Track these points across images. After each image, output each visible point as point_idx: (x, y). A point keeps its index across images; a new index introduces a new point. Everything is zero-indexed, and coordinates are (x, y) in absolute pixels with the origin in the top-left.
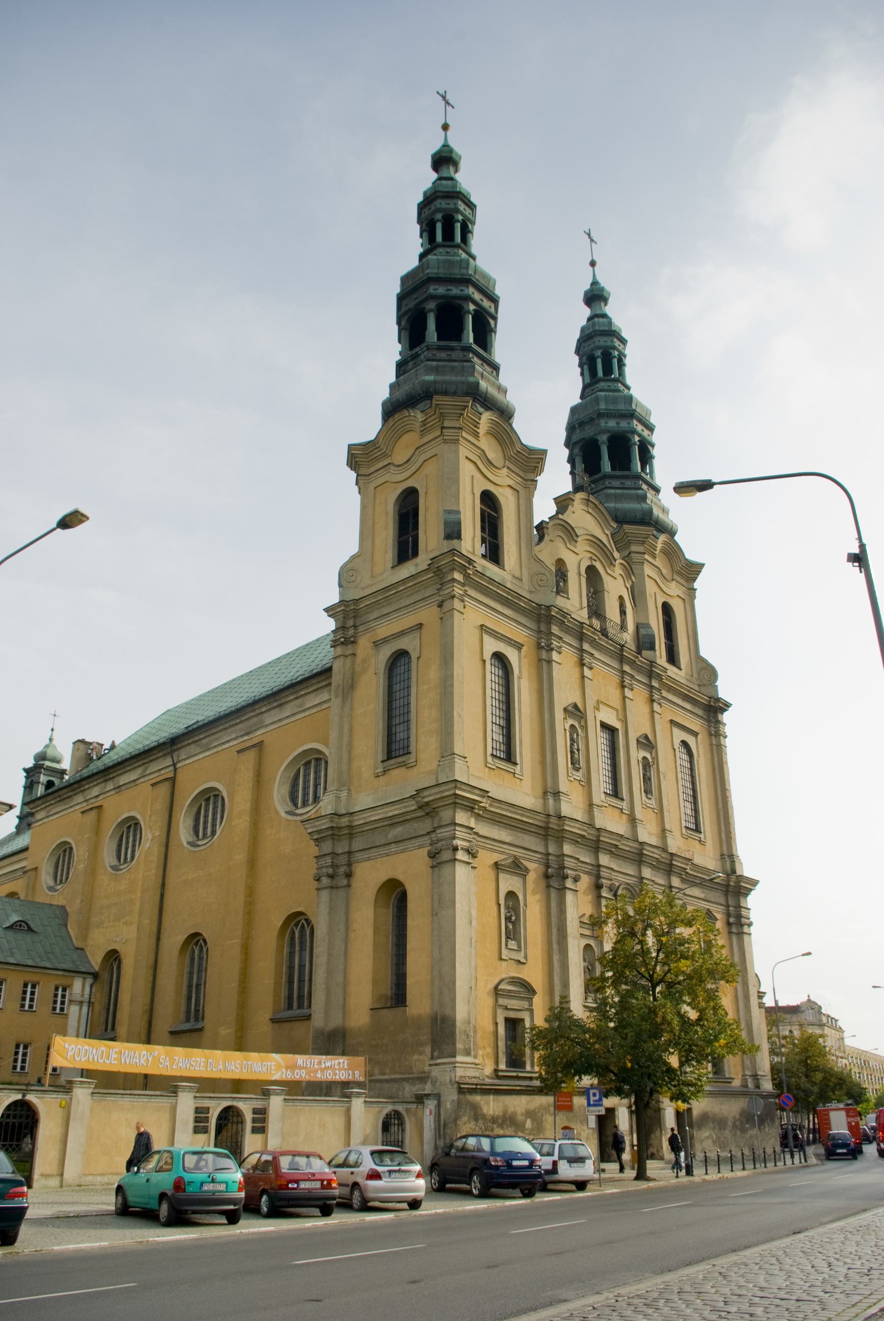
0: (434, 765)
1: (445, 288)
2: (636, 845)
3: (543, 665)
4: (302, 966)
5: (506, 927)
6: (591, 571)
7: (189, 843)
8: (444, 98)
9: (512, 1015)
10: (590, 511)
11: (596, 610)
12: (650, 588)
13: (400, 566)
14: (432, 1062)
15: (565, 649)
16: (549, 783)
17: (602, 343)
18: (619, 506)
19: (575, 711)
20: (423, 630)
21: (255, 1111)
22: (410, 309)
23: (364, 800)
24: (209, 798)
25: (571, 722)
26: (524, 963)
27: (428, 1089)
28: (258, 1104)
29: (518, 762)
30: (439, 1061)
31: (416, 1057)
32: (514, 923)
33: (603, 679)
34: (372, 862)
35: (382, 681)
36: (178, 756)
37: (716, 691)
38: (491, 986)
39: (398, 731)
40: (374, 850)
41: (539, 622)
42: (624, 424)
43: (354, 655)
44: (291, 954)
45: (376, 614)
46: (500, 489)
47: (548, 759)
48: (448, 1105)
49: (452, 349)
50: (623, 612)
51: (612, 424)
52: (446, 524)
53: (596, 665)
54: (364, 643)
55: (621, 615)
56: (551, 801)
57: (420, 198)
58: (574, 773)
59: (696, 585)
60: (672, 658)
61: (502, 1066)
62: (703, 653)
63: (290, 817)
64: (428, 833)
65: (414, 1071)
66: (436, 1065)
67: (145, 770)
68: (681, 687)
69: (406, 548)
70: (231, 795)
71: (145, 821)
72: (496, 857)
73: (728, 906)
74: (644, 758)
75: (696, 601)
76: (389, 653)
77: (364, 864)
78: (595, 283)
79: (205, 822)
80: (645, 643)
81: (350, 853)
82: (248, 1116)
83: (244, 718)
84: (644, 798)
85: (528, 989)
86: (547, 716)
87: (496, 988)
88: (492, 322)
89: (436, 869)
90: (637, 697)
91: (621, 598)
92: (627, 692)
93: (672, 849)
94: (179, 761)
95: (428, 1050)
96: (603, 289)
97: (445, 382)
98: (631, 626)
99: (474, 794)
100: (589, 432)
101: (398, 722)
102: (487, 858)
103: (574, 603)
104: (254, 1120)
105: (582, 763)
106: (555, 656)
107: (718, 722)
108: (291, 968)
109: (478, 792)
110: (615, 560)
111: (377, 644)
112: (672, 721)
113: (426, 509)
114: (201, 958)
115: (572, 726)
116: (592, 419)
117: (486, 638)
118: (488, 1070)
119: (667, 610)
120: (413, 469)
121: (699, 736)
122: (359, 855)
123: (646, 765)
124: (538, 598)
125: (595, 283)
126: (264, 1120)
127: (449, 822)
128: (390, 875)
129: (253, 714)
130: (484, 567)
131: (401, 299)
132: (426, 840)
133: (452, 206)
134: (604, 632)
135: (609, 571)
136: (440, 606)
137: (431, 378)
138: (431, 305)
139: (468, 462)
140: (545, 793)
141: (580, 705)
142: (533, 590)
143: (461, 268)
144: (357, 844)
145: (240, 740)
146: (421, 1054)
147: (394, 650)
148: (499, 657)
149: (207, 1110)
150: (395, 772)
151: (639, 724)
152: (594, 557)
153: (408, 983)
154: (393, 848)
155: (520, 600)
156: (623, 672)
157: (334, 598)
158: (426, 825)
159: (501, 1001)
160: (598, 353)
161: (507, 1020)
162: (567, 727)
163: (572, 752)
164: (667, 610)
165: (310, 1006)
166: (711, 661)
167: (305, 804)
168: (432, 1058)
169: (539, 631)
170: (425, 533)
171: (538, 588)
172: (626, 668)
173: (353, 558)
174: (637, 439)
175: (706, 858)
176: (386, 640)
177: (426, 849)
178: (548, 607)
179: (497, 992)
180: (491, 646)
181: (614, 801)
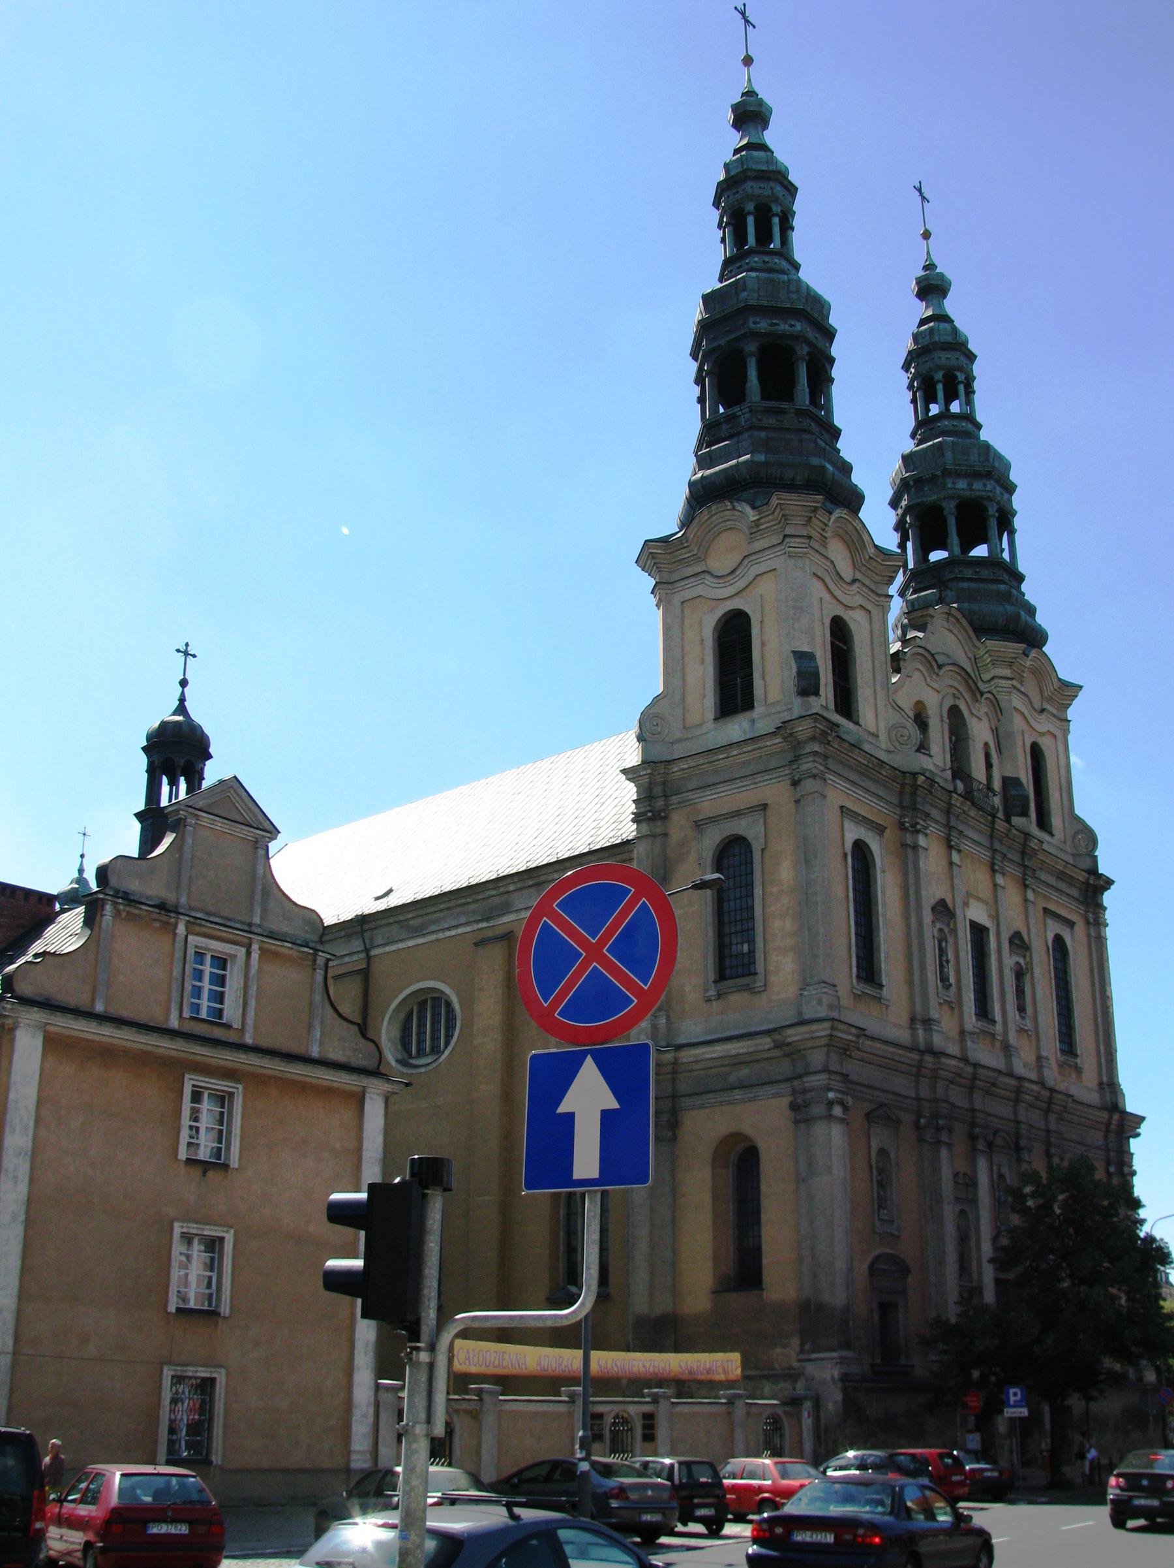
0: (791, 991)
2: (1014, 1082)
3: (907, 852)
5: (878, 1193)
6: (954, 712)
7: (398, 1061)
10: (951, 627)
12: (1018, 723)
13: (728, 719)
14: (802, 1357)
16: (918, 1008)
17: (943, 362)
19: (943, 910)
20: (769, 811)
22: (720, 346)
25: (938, 925)
26: (898, 1237)
27: (800, 1388)
28: (647, 1409)
29: (884, 983)
30: (814, 1356)
31: (778, 1350)
34: (707, 1111)
39: (734, 941)
40: (710, 1095)
42: (978, 485)
43: (666, 835)
46: (851, 613)
47: (916, 977)
48: (830, 1407)
49: (783, 412)
50: (989, 766)
53: (967, 846)
56: (921, 1032)
57: (722, 176)
59: (1071, 713)
60: (1043, 822)
61: (878, 1361)
62: (1078, 811)
64: (788, 1080)
65: (777, 1366)
66: (810, 1360)
70: (468, 1002)
73: (1108, 1151)
74: (1018, 963)
75: (1069, 737)
76: (718, 838)
77: (694, 1113)
78: (929, 267)
83: (481, 897)
84: (1018, 1017)
85: (903, 1269)
86: (913, 920)
87: (871, 1267)
88: (828, 367)
89: (803, 1126)
91: (986, 744)
92: (1000, 880)
93: (1050, 1083)
95: (795, 1342)
96: (941, 276)
98: (997, 785)
101: (733, 930)
103: (938, 759)
104: (645, 1427)
105: (952, 980)
107: (1100, 908)
109: (853, 1030)
110: (982, 694)
111: (699, 826)
112: (1045, 910)
113: (763, 644)
119: (1036, 753)
120: (741, 584)
121: (1076, 927)
122: (688, 1101)
123: (1019, 974)
124: (897, 761)
125: (929, 267)
127: (820, 1068)
129: (494, 892)
131: (705, 328)
132: (785, 1088)
133: (768, 192)
134: (968, 796)
135: (974, 711)
136: (795, 783)
138: (752, 347)
139: (815, 580)
140: (913, 1020)
141: (949, 902)
142: (892, 749)
143: (789, 292)
145: (475, 927)
146: (785, 1346)
148: (860, 847)
149: (600, 1416)
150: (735, 998)
153: (764, 1261)
154: (737, 1094)
156: (995, 851)
157: (633, 757)
160: (939, 376)
162: (936, 930)
163: (941, 965)
164: (1036, 753)
166: (1089, 823)
168: (802, 1351)
169: (902, 807)
170: (763, 678)
171: (896, 744)
173: (657, 700)
174: (996, 507)
175: (1085, 1089)
176: (713, 820)
177: (785, 1101)
180: (853, 833)
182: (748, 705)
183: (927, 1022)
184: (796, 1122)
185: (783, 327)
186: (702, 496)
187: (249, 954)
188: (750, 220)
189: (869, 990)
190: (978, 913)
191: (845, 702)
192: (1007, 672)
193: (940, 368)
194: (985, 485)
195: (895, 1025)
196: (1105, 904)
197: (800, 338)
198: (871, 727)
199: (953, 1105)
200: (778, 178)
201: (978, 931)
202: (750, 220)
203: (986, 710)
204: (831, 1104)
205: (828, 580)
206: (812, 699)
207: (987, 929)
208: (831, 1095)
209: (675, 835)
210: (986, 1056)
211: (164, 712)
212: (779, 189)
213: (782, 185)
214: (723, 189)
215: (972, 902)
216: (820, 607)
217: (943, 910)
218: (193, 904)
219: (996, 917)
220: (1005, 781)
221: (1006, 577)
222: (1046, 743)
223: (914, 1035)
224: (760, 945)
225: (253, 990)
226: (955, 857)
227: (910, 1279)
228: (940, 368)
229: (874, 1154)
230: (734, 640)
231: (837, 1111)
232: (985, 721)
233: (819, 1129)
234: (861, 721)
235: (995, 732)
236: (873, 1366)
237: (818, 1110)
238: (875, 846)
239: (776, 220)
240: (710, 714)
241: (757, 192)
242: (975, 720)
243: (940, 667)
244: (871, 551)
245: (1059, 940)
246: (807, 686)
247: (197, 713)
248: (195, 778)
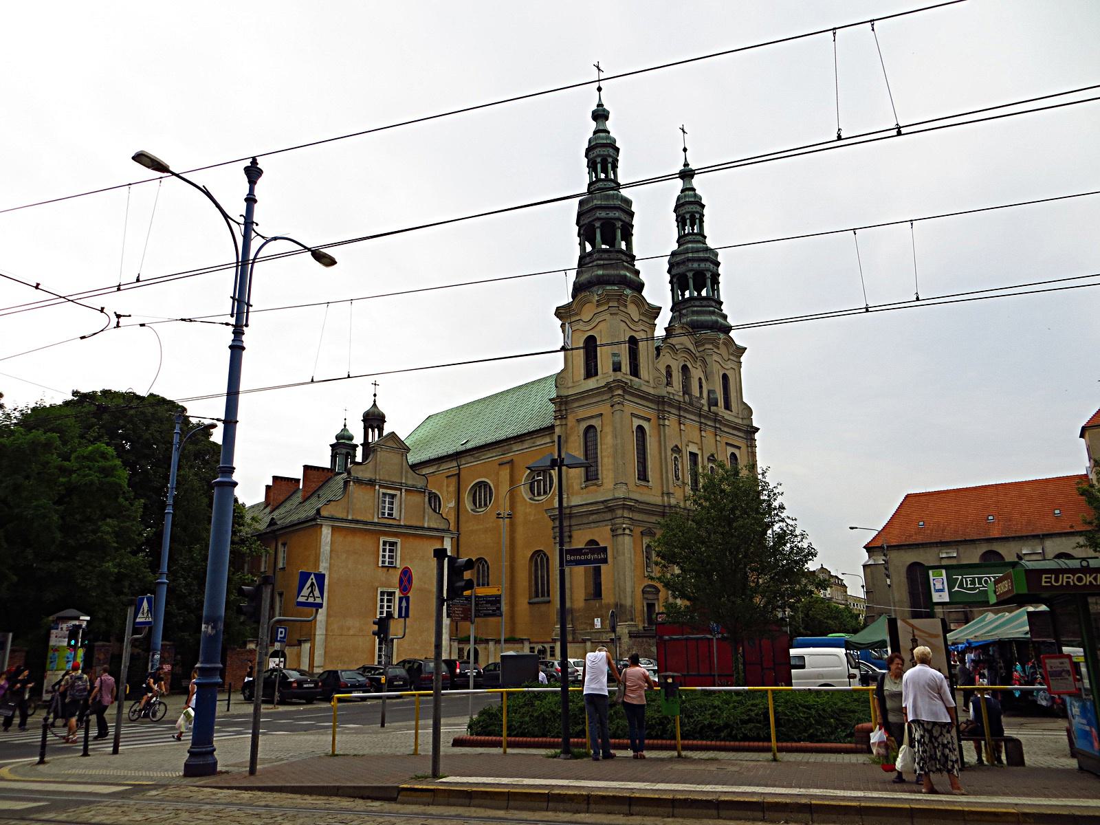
4: (542, 577)
6: (685, 368)
7: (471, 510)
8: (598, 67)
9: (650, 602)
11: (686, 390)
12: (716, 367)
15: (672, 417)
16: (665, 489)
17: (690, 210)
19: (676, 449)
21: (551, 647)
22: (585, 224)
23: (575, 501)
24: (481, 486)
25: (674, 455)
32: (649, 559)
33: (691, 428)
35: (582, 440)
36: (460, 462)
38: (641, 590)
41: (658, 404)
42: (702, 265)
43: (566, 424)
44: (536, 570)
45: (576, 404)
46: (638, 333)
50: (701, 387)
51: (695, 265)
52: (614, 363)
54: (571, 419)
56: (666, 498)
60: (728, 406)
61: (646, 625)
63: (531, 502)
64: (610, 520)
67: (439, 467)
69: (591, 371)
70: (497, 486)
71: (442, 495)
72: (641, 529)
74: (712, 467)
76: (585, 426)
79: (480, 499)
80: (713, 402)
81: (570, 526)
82: (548, 650)
87: (643, 590)
88: (631, 229)
90: (708, 435)
91: (700, 379)
94: (461, 465)
97: (608, 275)
100: (682, 269)
102: (638, 530)
104: (551, 651)
106: (667, 422)
108: (536, 577)
111: (579, 421)
112: (727, 444)
114: (483, 571)
115: (675, 457)
116: (684, 262)
117: (634, 419)
118: (641, 627)
119: (725, 377)
120: (593, 325)
126: (554, 651)
128: (591, 538)
130: (631, 380)
132: (609, 523)
133: (606, 153)
137: (600, 272)
140: (663, 493)
144: (574, 522)
145: (499, 457)
147: (588, 424)
148: (640, 428)
151: (710, 448)
152: (686, 360)
154: (592, 525)
156: (701, 423)
158: (609, 516)
159: (646, 596)
161: (648, 604)
162: (673, 458)
164: (725, 377)
165: (548, 595)
167: (539, 494)
172: (703, 420)
177: (609, 527)
178: (663, 397)
179: (643, 592)
180: (637, 422)
182: (596, 374)
183: (668, 494)
184: (613, 536)
185: (611, 214)
186: (578, 289)
187: (401, 493)
189: (643, 483)
190: (693, 449)
191: (635, 371)
192: (711, 346)
193: (689, 211)
197: (619, 219)
198: (647, 378)
201: (693, 456)
203: (700, 364)
204: (624, 529)
205: (628, 323)
206: (618, 373)
208: (624, 526)
209: (570, 424)
211: (367, 406)
212: (611, 150)
213: (612, 148)
214: (588, 151)
215: (690, 444)
217: (676, 449)
218: (381, 478)
219: (701, 449)
220: (709, 392)
221: (714, 304)
222: (730, 374)
223: (663, 500)
224: (600, 468)
225: (403, 506)
226: (682, 427)
227: (660, 593)
228: (689, 211)
229: (644, 547)
230: (591, 345)
231: (627, 531)
232: (700, 368)
233: (620, 538)
234: (642, 377)
235: (705, 373)
236: (644, 627)
237: (620, 532)
238: (645, 425)
239: (610, 165)
240: (583, 378)
241: (602, 153)
243: (677, 351)
244: (646, 307)
246: (617, 368)
247: (382, 407)
248: (381, 430)
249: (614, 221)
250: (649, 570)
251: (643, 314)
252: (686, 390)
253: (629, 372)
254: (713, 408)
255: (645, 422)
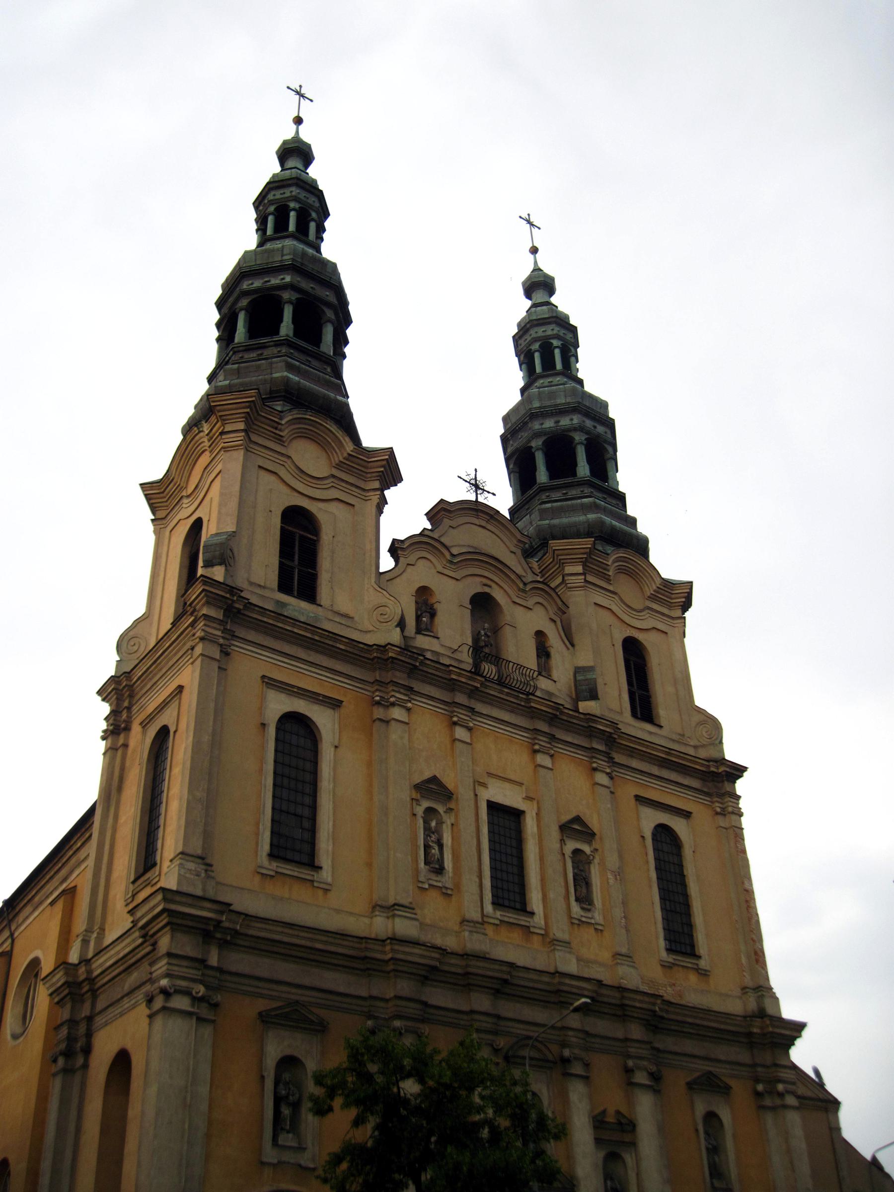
1: (262, 281)
10: (483, 523)
17: (540, 334)
18: (556, 522)
25: (426, 804)
37: (722, 751)
42: (565, 422)
46: (321, 505)
49: (264, 347)
50: (543, 652)
51: (549, 424)
55: (538, 656)
58: (433, 876)
68: (654, 749)
72: (262, 1005)
78: (537, 269)
84: (576, 909)
91: (540, 635)
99: (202, 908)
112: (638, 798)
115: (430, 811)
142: (371, 628)
143: (282, 256)
155: (336, 640)
162: (420, 810)
163: (427, 847)
166: (711, 711)
180: (279, 705)
181: (511, 917)
188: (537, 356)
194: (572, 420)
195: (338, 911)
196: (738, 793)
199: (425, 1004)
200: (563, 322)
202: (537, 356)
207: (523, 812)
210: (510, 949)
216: (275, 498)
242: (519, 611)
245: (663, 834)
249: (278, 293)
250: (286, 1139)
251: (339, 466)
252: (486, 648)
253: (275, 585)
254: (585, 706)
255: (316, 708)
